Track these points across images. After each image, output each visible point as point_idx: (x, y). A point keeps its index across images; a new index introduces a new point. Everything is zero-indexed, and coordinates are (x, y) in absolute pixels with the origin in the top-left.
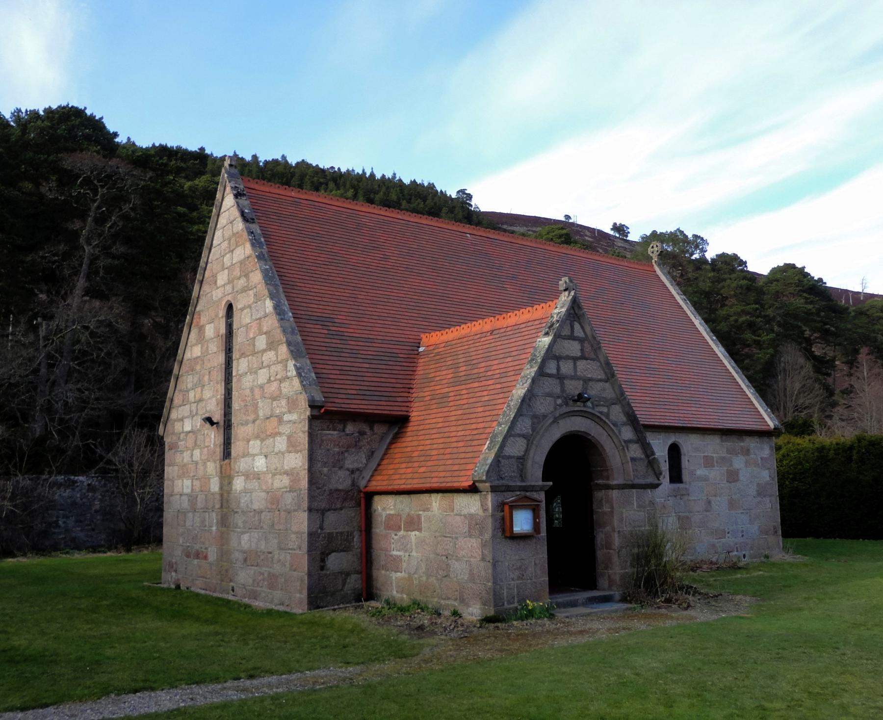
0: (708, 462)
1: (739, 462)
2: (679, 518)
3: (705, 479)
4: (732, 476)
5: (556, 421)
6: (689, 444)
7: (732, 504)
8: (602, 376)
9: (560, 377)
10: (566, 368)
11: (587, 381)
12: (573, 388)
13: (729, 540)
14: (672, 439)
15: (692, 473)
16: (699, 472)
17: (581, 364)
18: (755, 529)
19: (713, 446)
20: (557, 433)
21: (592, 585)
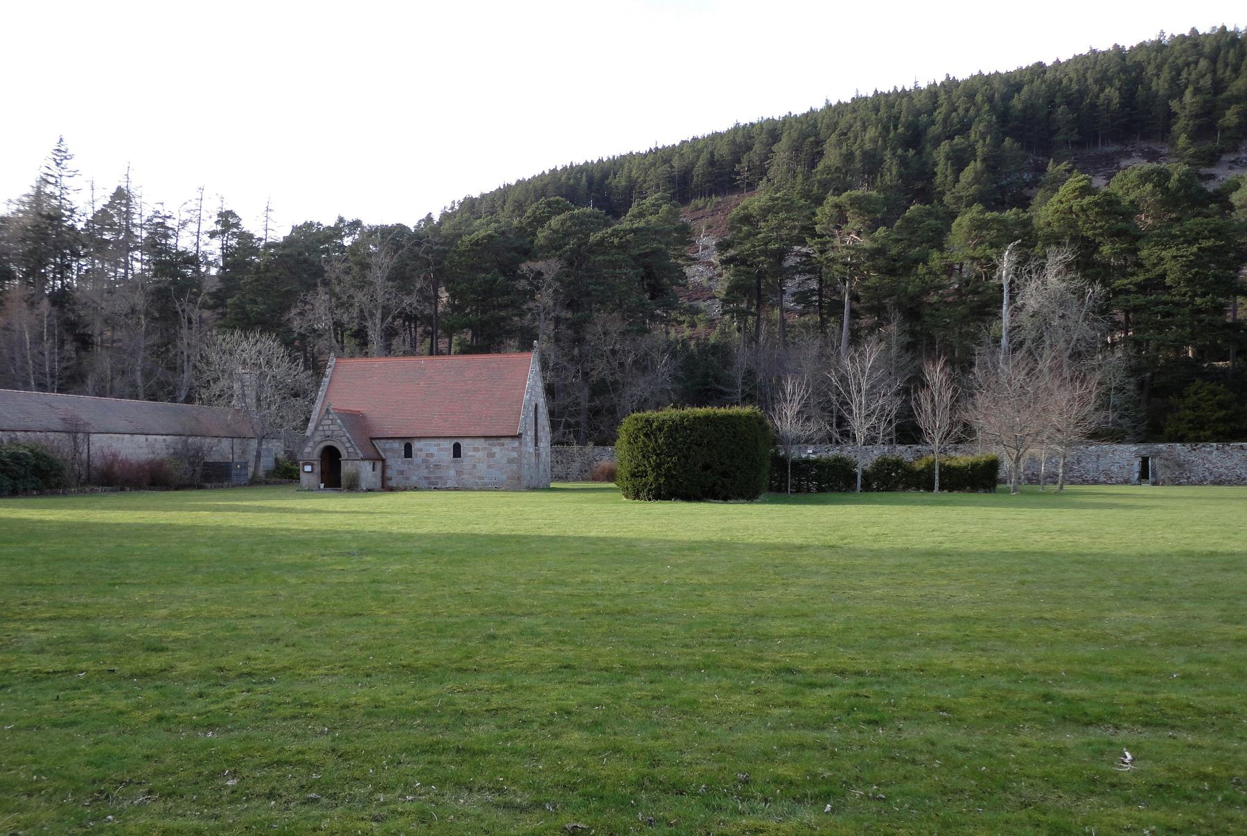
0: (476, 450)
1: (496, 449)
2: (457, 471)
3: (474, 456)
4: (491, 455)
5: (322, 442)
6: (463, 443)
7: (489, 467)
8: (338, 428)
9: (324, 430)
10: (326, 428)
11: (333, 431)
12: (328, 433)
13: (486, 480)
14: (455, 441)
15: (464, 454)
16: (469, 454)
17: (331, 427)
18: (504, 477)
19: (480, 443)
20: (322, 446)
21: (340, 486)
